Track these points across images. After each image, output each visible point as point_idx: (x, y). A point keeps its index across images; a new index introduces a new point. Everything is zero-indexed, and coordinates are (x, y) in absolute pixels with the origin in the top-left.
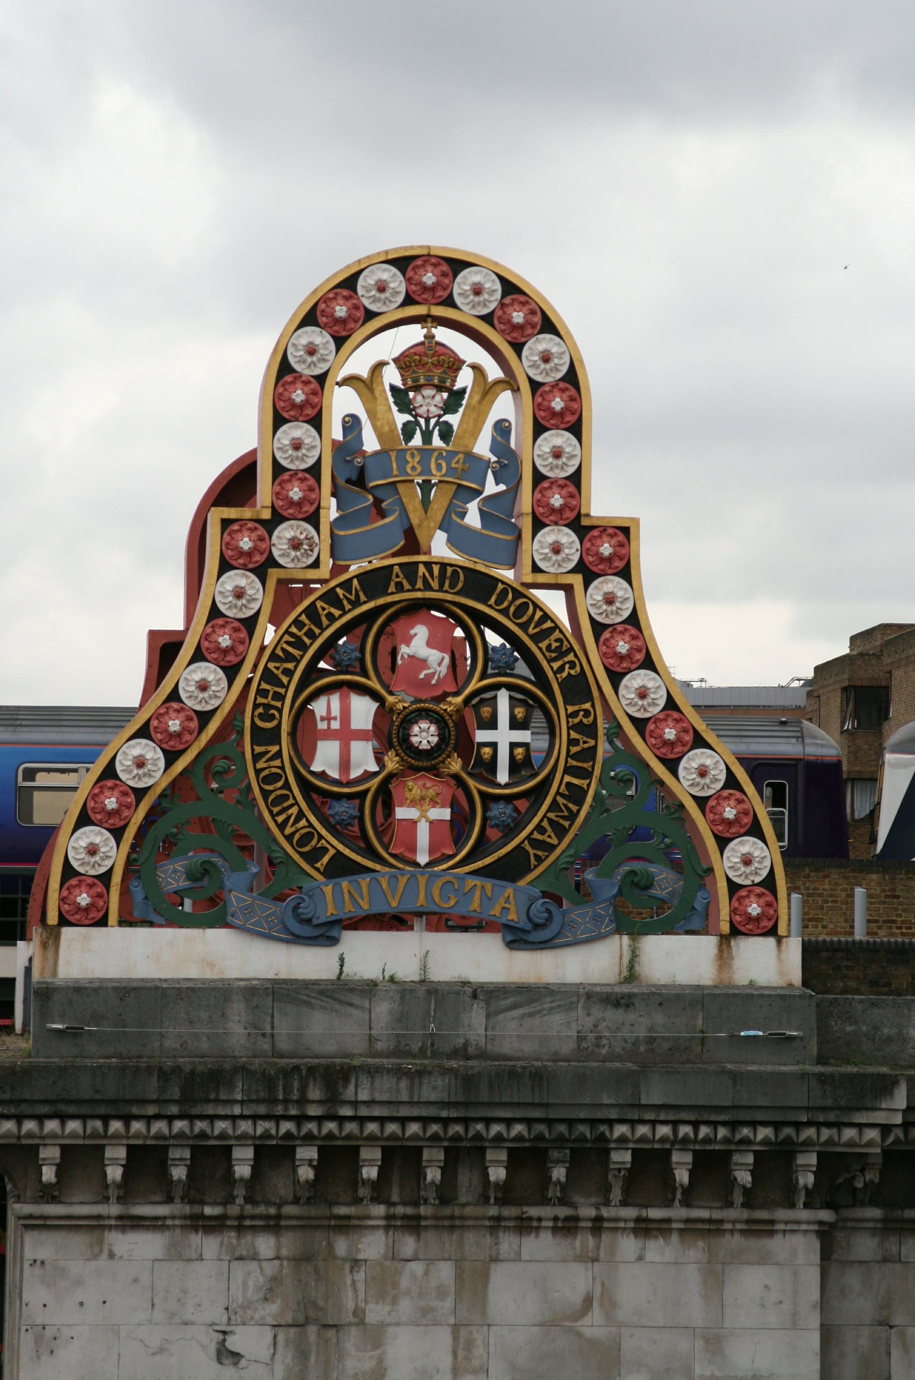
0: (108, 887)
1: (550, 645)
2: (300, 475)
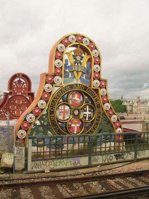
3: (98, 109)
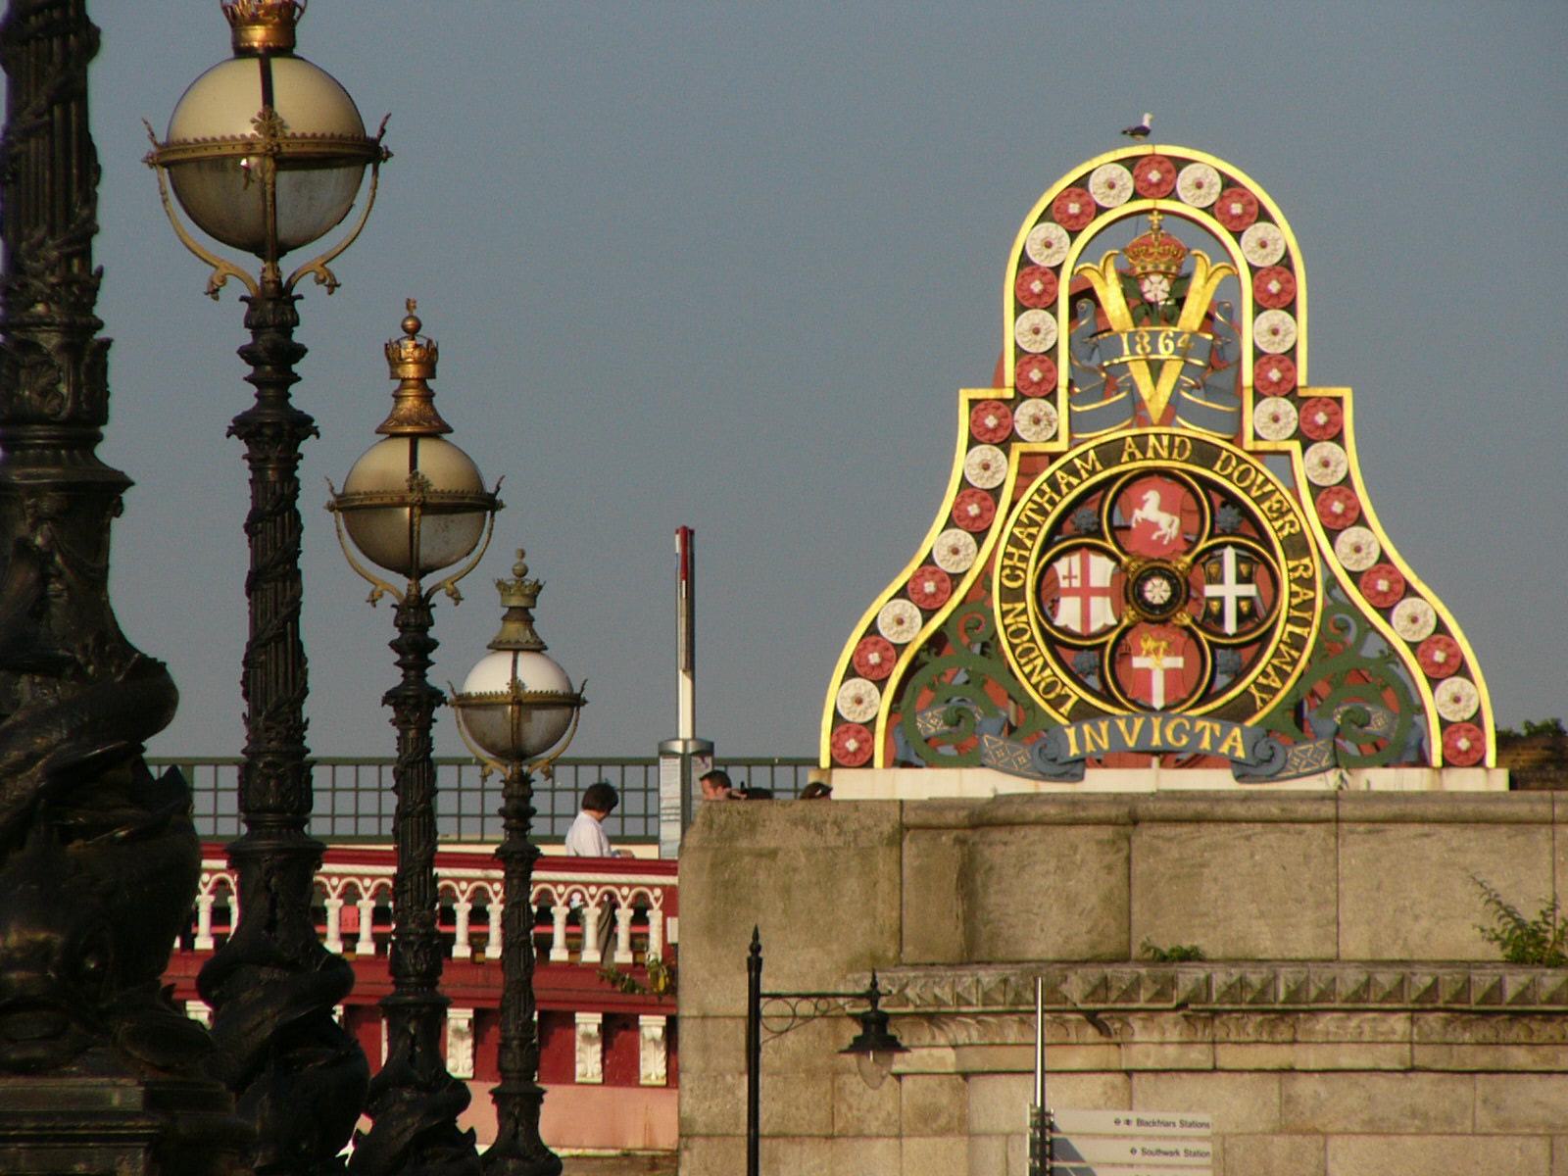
0: (873, 734)
2: (1040, 357)
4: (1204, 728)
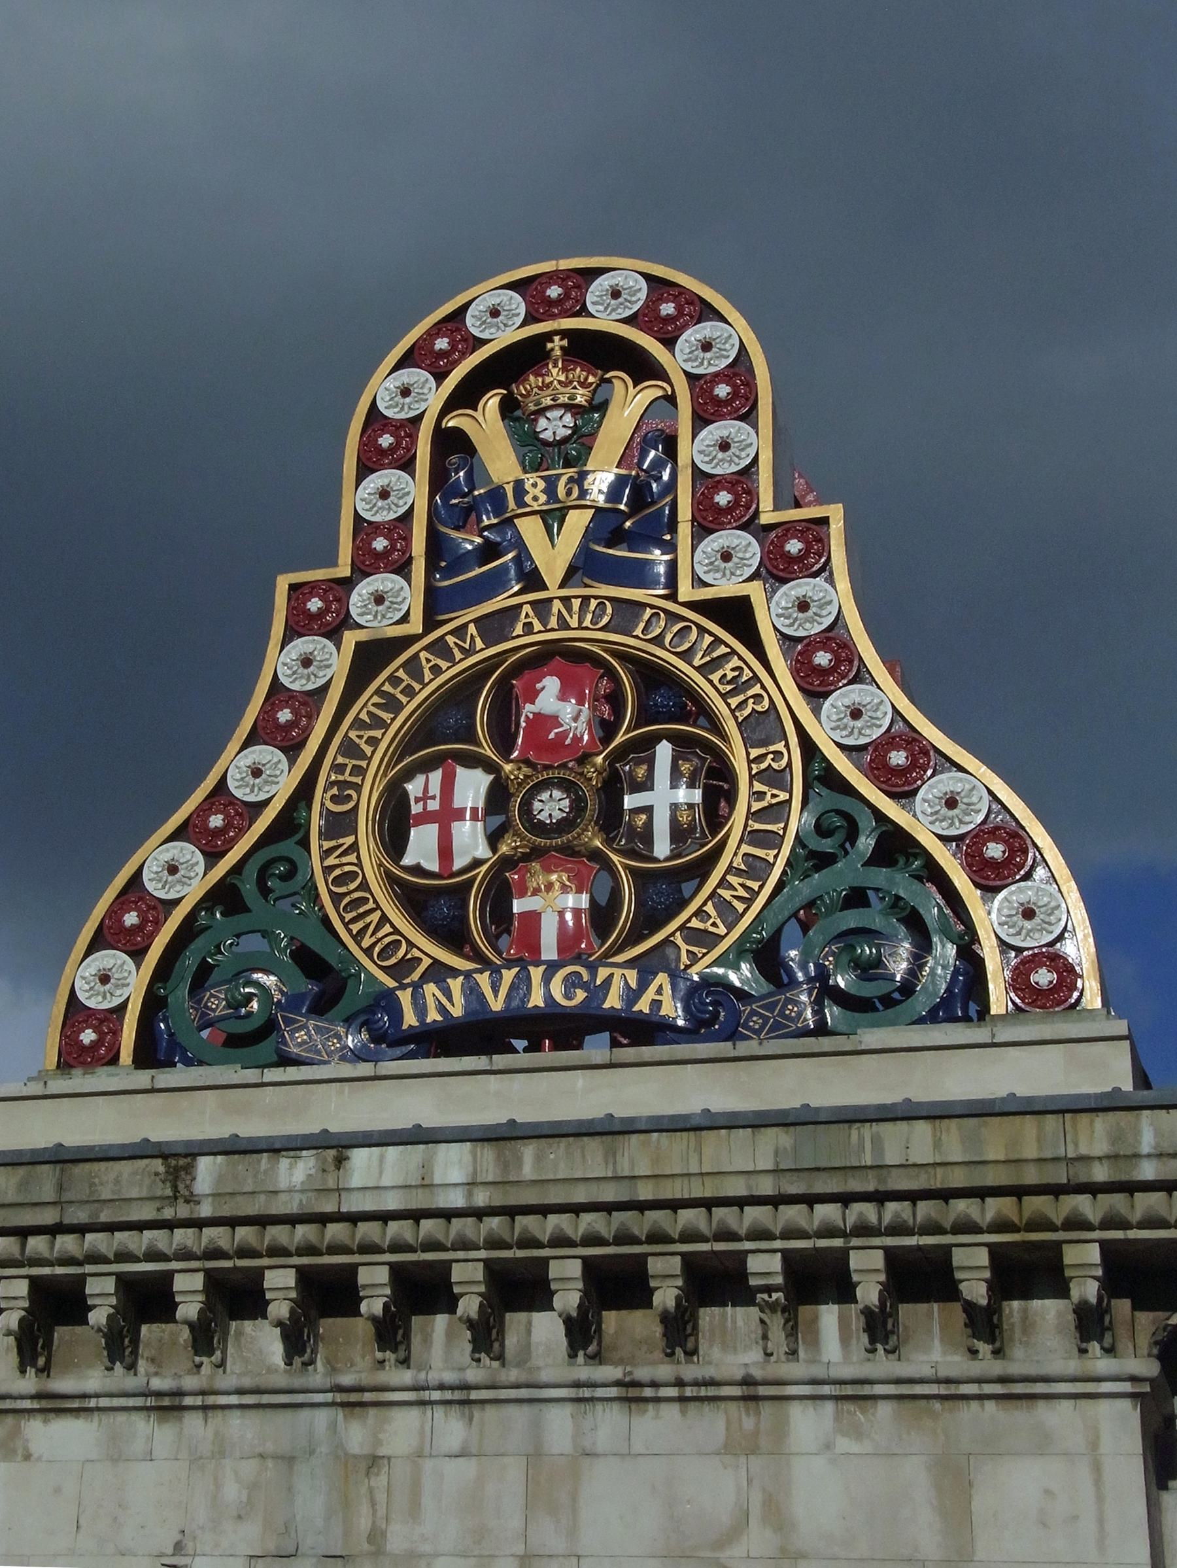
1: (725, 675)
3: (754, 753)
4: (608, 980)
